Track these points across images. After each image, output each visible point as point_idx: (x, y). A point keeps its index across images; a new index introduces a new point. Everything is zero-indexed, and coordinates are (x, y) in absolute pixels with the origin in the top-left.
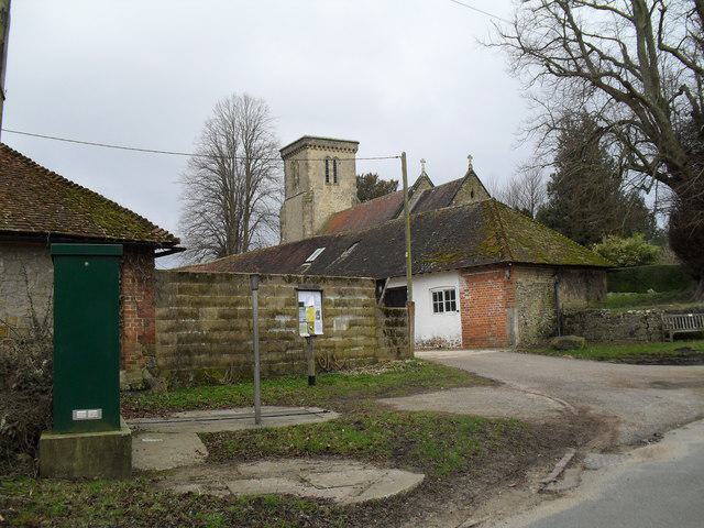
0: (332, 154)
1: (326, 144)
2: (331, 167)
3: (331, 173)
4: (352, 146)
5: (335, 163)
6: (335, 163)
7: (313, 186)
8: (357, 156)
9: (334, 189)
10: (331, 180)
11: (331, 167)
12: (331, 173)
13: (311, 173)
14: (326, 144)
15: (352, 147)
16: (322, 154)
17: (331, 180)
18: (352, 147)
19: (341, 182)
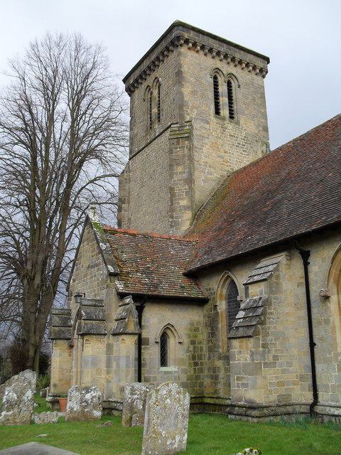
0: (227, 68)
1: (216, 45)
2: (223, 89)
3: (224, 100)
4: (258, 63)
5: (229, 84)
6: (229, 84)
7: (191, 114)
8: (267, 81)
9: (230, 126)
10: (225, 112)
11: (223, 89)
12: (224, 100)
13: (186, 90)
14: (216, 45)
15: (260, 63)
16: (210, 63)
17: (225, 112)
18: (260, 63)
19: (242, 120)
